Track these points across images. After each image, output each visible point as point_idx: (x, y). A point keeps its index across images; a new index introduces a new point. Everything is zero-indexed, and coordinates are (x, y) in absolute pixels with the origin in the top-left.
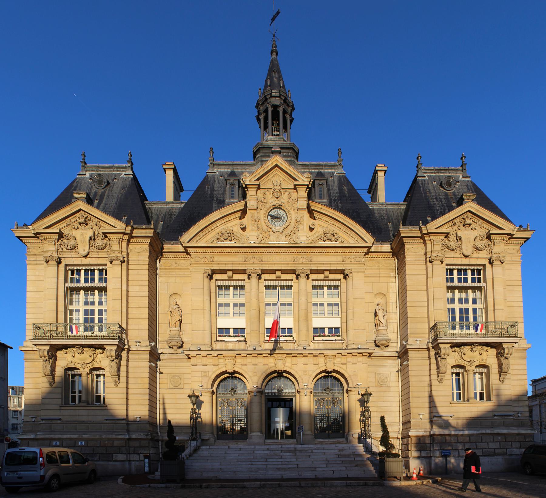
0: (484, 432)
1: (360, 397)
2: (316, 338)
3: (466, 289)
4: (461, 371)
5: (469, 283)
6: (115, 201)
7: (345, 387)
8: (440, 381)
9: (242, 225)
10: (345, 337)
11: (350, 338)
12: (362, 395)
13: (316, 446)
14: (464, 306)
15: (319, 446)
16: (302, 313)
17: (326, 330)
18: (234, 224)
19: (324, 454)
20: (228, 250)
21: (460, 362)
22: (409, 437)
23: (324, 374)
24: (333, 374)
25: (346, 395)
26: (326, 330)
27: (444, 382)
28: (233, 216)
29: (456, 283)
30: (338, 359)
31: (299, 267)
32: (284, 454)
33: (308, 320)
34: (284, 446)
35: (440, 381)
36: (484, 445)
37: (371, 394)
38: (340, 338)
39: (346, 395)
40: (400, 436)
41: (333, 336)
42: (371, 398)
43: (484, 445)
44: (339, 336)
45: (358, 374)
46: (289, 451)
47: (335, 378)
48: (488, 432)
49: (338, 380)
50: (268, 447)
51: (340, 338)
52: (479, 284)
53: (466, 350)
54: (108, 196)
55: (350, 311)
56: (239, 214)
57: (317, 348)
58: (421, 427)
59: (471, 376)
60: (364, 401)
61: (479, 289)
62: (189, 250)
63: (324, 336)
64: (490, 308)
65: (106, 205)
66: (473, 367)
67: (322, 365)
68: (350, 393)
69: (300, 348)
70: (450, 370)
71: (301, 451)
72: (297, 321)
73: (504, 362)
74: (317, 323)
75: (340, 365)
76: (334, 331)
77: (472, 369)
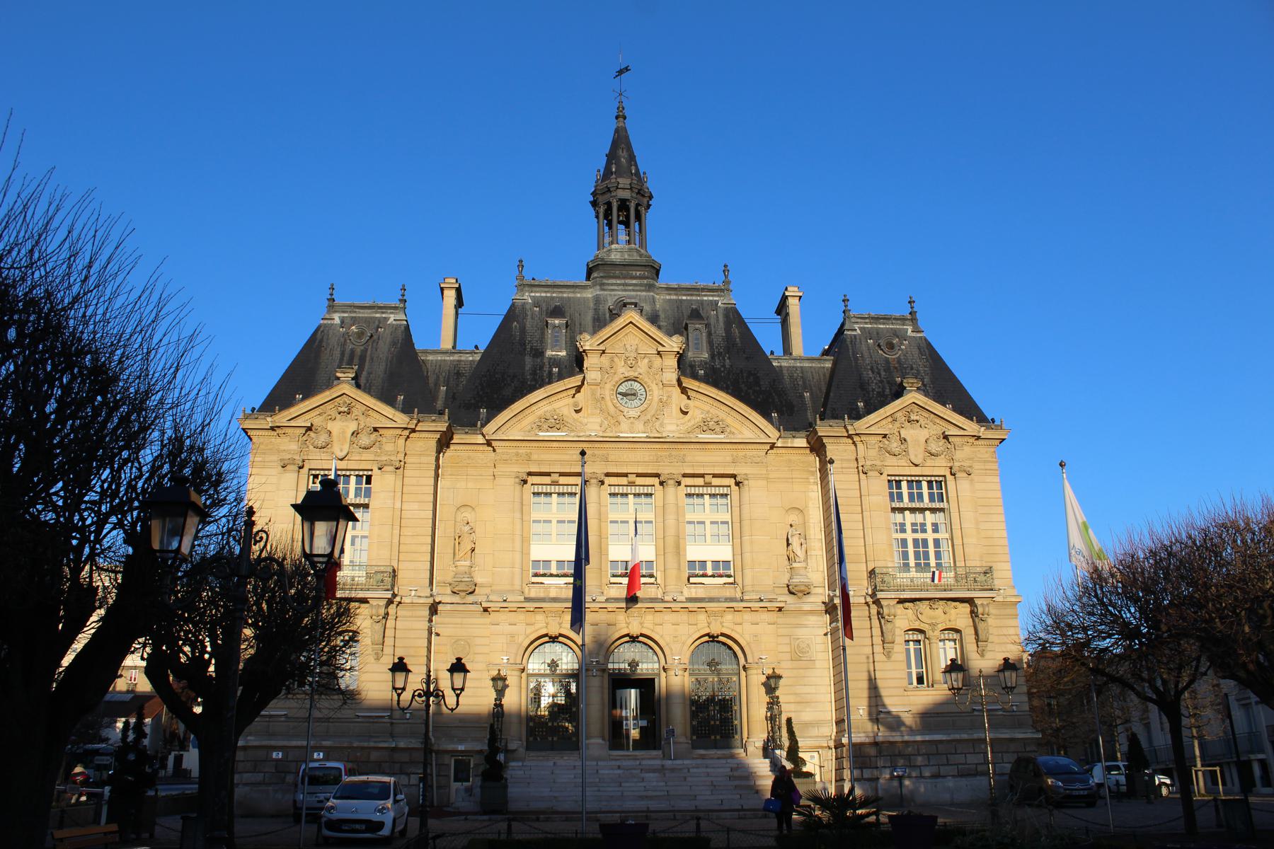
0: (957, 737)
1: (763, 679)
2: (692, 580)
3: (922, 510)
4: (920, 637)
5: (926, 502)
6: (382, 367)
7: (742, 661)
8: (888, 655)
9: (576, 404)
10: (739, 580)
11: (748, 581)
12: (768, 678)
13: (694, 762)
14: (920, 536)
15: (699, 761)
16: (670, 541)
17: (709, 565)
18: (563, 406)
19: (708, 775)
20: (555, 444)
21: (917, 625)
22: (843, 745)
23: (706, 638)
24: (721, 638)
25: (743, 674)
26: (709, 565)
27: (894, 657)
28: (564, 394)
29: (906, 502)
30: (729, 617)
31: (664, 470)
32: (647, 775)
33: (679, 550)
34: (644, 762)
35: (888, 655)
36: (960, 758)
37: (780, 677)
38: (731, 580)
39: (743, 674)
40: (832, 744)
41: (721, 576)
42: (782, 682)
43: (960, 758)
44: (729, 576)
45: (762, 641)
46: (654, 771)
47: (724, 644)
48: (965, 736)
49: (730, 648)
50: (618, 763)
51: (731, 580)
52: (941, 505)
53: (923, 606)
54: (372, 359)
55: (745, 538)
56: (573, 391)
57: (694, 595)
58: (862, 729)
59: (934, 646)
60: (771, 683)
61: (942, 510)
62: (494, 444)
63: (704, 575)
64: (958, 541)
65: (369, 374)
66: (937, 633)
67: (703, 624)
68: (749, 672)
69: (667, 598)
70: (900, 638)
71: (673, 770)
72: (662, 551)
73: (981, 626)
74: (694, 552)
75: (731, 625)
76: (721, 569)
77: (934, 634)
